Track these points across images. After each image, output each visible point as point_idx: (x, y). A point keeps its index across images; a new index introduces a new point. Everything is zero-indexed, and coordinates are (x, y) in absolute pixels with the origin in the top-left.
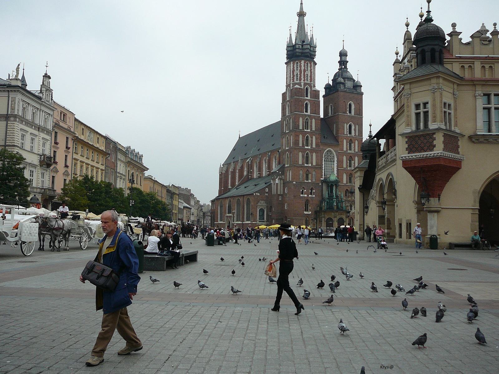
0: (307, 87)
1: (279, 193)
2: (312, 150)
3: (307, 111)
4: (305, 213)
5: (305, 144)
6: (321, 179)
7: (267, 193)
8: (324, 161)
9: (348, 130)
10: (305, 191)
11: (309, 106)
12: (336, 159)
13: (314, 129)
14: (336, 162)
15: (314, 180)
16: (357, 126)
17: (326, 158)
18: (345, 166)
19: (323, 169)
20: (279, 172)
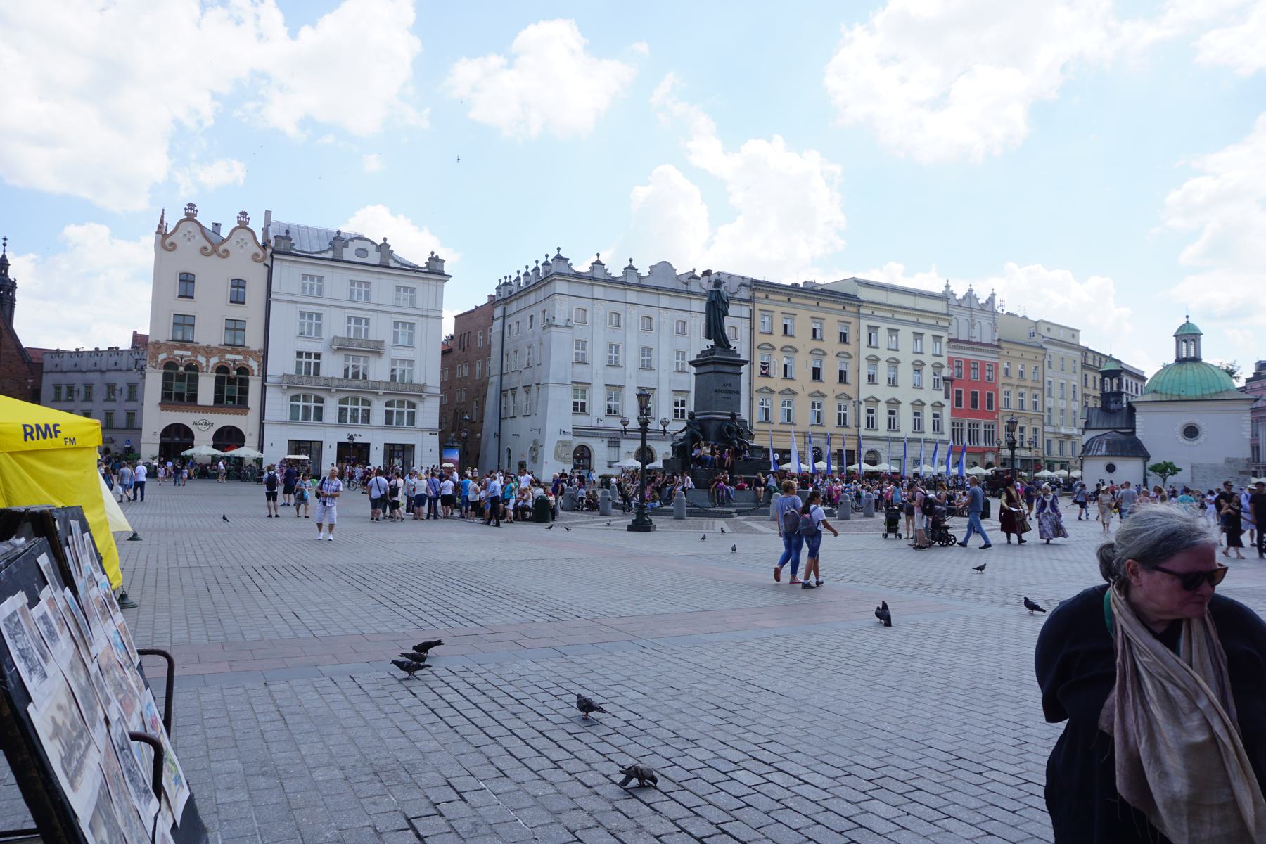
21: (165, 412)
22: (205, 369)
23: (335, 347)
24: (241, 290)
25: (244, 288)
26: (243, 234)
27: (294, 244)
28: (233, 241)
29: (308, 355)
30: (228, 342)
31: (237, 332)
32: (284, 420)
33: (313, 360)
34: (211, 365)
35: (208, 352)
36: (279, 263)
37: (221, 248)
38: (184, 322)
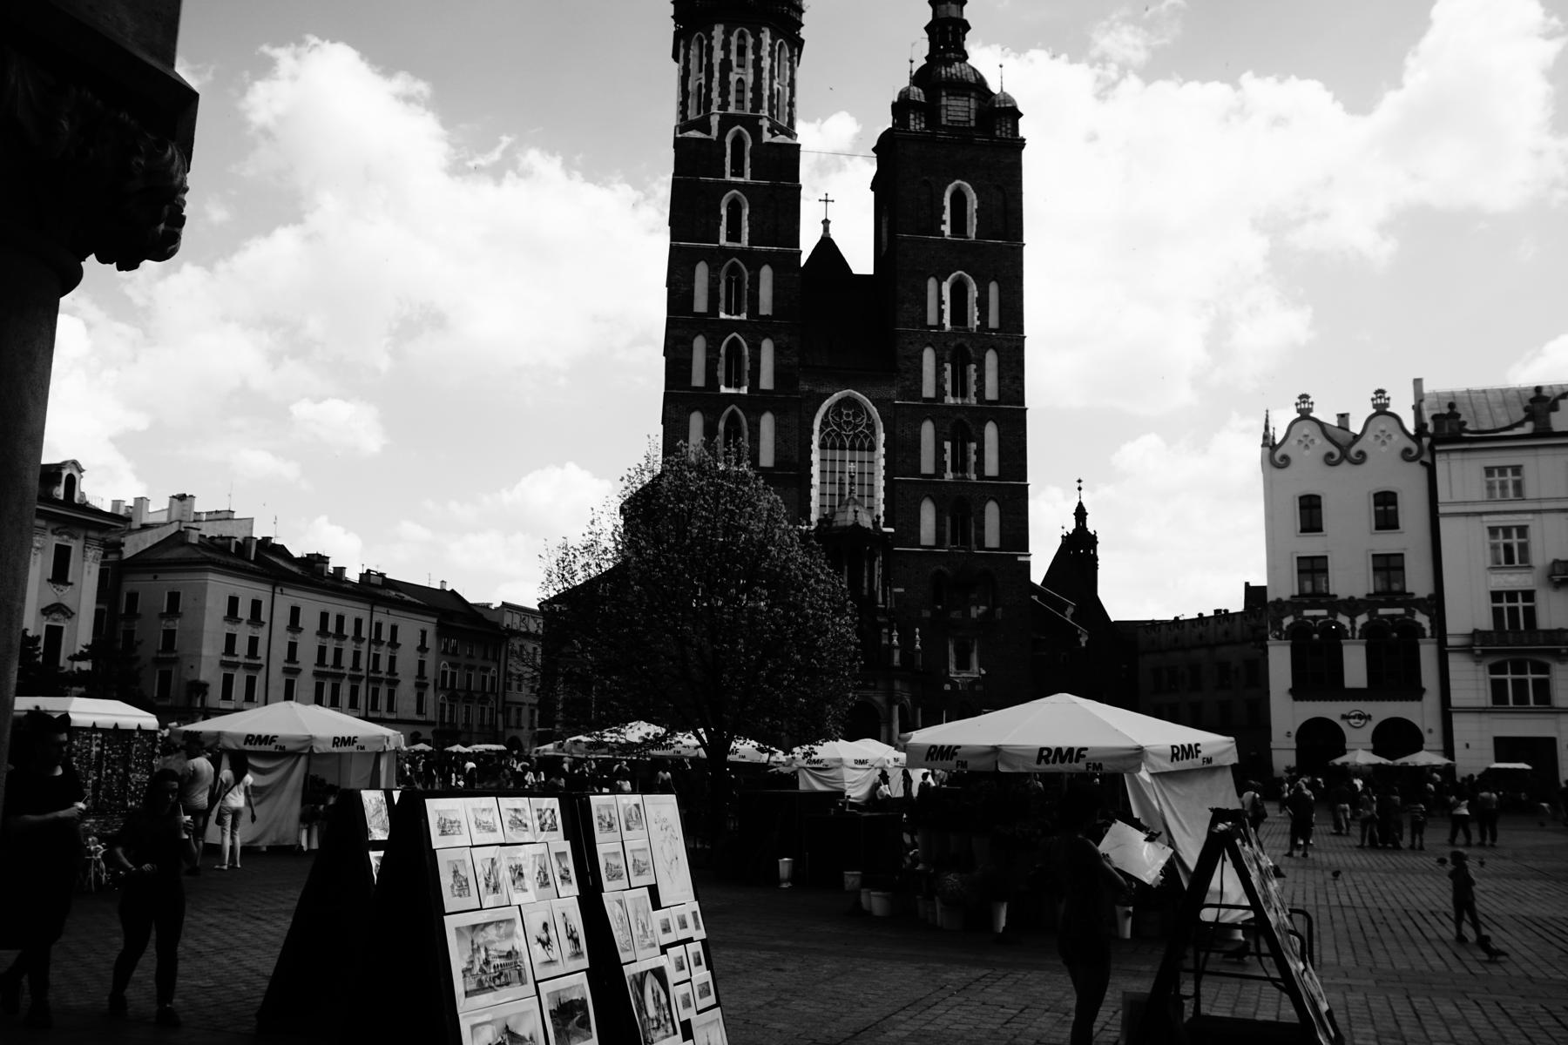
0: (739, 131)
2: (757, 403)
3: (734, 235)
8: (822, 446)
11: (746, 212)
12: (882, 437)
13: (766, 308)
14: (882, 450)
16: (993, 288)
17: (828, 434)
21: (1299, 703)
22: (1350, 634)
23: (1557, 578)
24: (1390, 508)
25: (1395, 503)
26: (1383, 423)
27: (1464, 423)
28: (1369, 437)
29: (1512, 596)
30: (1379, 588)
31: (1392, 573)
32: (1483, 704)
33: (1520, 604)
34: (1358, 626)
35: (1352, 606)
36: (1444, 456)
37: (1353, 451)
38: (1312, 568)
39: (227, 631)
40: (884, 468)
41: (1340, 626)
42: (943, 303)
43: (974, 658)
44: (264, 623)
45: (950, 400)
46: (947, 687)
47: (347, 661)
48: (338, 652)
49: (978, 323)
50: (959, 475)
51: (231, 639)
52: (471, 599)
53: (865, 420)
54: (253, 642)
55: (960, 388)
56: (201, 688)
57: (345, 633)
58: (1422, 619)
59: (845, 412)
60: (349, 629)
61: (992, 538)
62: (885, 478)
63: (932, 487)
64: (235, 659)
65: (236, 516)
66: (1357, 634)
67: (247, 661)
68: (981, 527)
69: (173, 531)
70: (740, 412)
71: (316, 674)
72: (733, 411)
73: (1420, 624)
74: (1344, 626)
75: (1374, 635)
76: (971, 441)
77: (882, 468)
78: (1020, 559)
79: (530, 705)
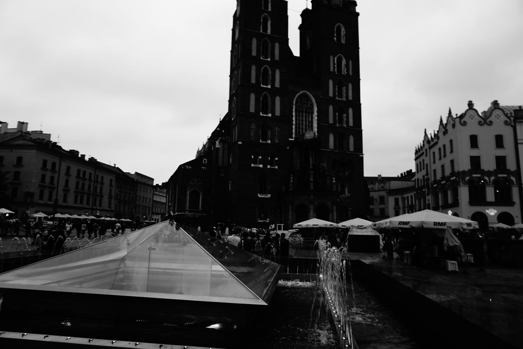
1: (220, 164)
2: (274, 92)
4: (260, 196)
5: (261, 79)
6: (290, 139)
7: (204, 165)
8: (296, 110)
9: (336, 66)
10: (260, 157)
11: (269, 23)
12: (316, 109)
13: (277, 58)
14: (316, 114)
15: (277, 141)
16: (351, 62)
18: (331, 121)
19: (294, 123)
20: (221, 130)
22: (489, 183)
34: (491, 180)
35: (489, 174)
36: (519, 124)
37: (488, 121)
39: (42, 173)
40: (317, 120)
41: (485, 180)
42: (335, 64)
43: (346, 190)
44: (57, 171)
45: (337, 98)
46: (338, 200)
47: (86, 188)
48: (83, 185)
49: (346, 73)
50: (341, 125)
51: (43, 177)
52: (125, 171)
53: (310, 103)
54: (52, 178)
55: (340, 96)
56: (30, 195)
57: (86, 177)
58: (513, 179)
59: (303, 99)
60: (87, 177)
61: (352, 149)
62: (317, 124)
63: (332, 128)
64: (45, 184)
65: (43, 133)
66: (491, 183)
67: (50, 185)
68: (348, 143)
69: (19, 135)
70: (268, 95)
71: (75, 192)
72: (266, 94)
73: (512, 180)
74: (487, 180)
75: (497, 184)
76: (344, 113)
77: (316, 120)
78: (360, 156)
79: (143, 206)
